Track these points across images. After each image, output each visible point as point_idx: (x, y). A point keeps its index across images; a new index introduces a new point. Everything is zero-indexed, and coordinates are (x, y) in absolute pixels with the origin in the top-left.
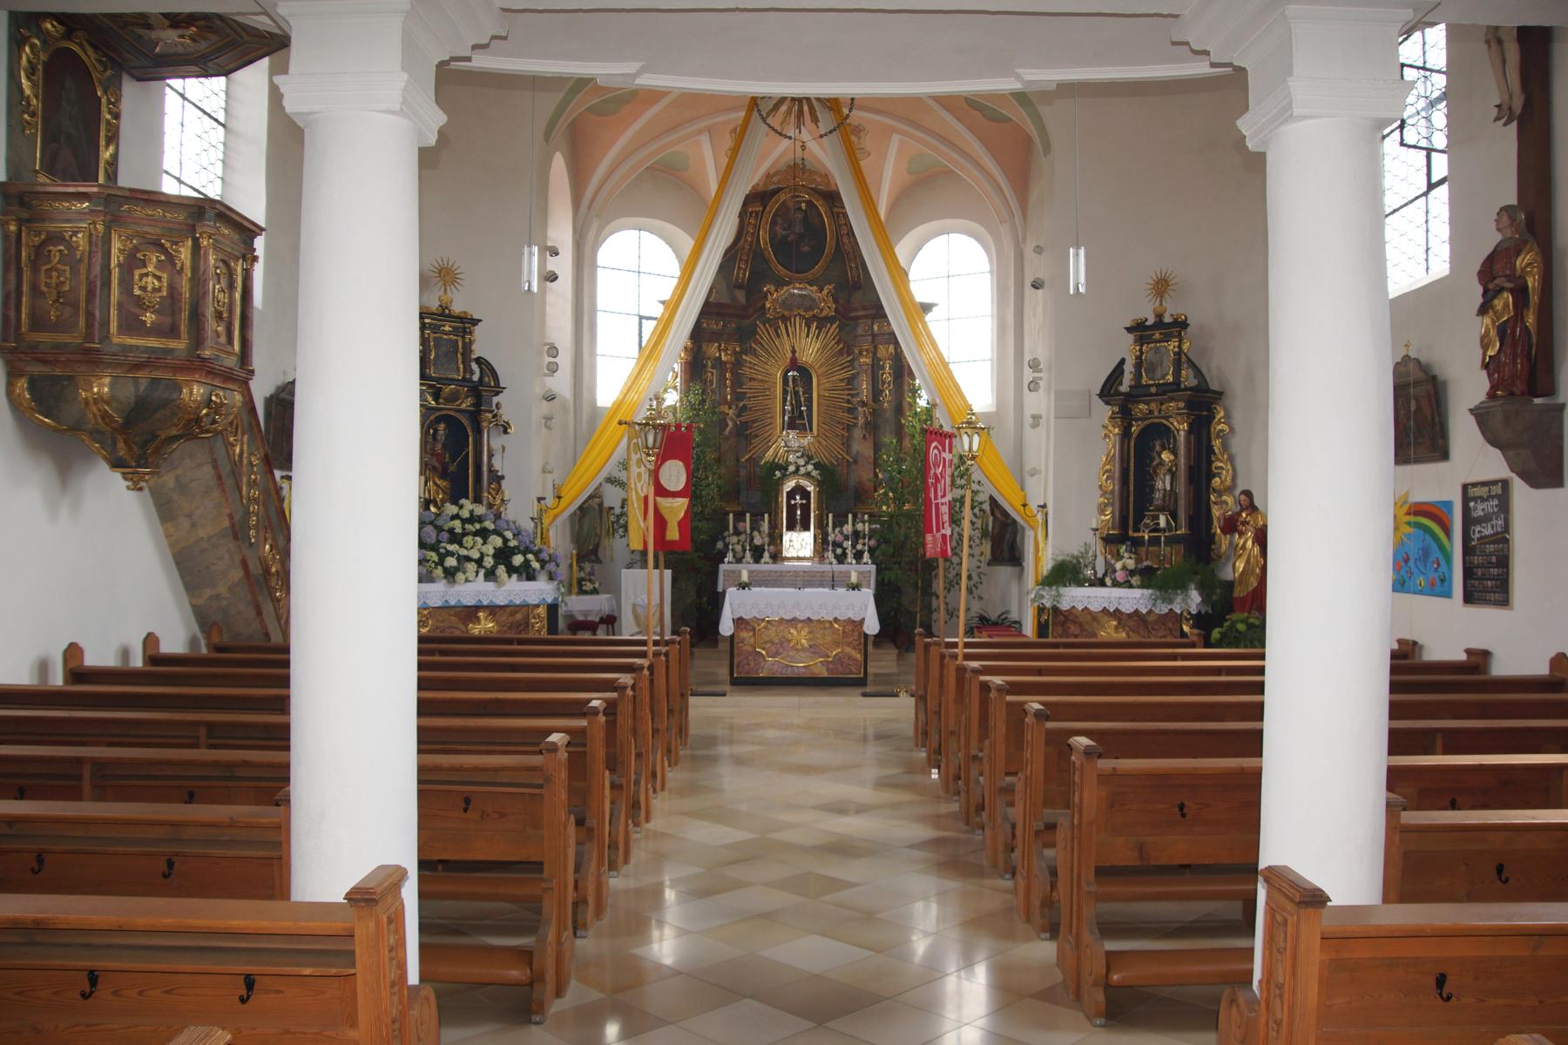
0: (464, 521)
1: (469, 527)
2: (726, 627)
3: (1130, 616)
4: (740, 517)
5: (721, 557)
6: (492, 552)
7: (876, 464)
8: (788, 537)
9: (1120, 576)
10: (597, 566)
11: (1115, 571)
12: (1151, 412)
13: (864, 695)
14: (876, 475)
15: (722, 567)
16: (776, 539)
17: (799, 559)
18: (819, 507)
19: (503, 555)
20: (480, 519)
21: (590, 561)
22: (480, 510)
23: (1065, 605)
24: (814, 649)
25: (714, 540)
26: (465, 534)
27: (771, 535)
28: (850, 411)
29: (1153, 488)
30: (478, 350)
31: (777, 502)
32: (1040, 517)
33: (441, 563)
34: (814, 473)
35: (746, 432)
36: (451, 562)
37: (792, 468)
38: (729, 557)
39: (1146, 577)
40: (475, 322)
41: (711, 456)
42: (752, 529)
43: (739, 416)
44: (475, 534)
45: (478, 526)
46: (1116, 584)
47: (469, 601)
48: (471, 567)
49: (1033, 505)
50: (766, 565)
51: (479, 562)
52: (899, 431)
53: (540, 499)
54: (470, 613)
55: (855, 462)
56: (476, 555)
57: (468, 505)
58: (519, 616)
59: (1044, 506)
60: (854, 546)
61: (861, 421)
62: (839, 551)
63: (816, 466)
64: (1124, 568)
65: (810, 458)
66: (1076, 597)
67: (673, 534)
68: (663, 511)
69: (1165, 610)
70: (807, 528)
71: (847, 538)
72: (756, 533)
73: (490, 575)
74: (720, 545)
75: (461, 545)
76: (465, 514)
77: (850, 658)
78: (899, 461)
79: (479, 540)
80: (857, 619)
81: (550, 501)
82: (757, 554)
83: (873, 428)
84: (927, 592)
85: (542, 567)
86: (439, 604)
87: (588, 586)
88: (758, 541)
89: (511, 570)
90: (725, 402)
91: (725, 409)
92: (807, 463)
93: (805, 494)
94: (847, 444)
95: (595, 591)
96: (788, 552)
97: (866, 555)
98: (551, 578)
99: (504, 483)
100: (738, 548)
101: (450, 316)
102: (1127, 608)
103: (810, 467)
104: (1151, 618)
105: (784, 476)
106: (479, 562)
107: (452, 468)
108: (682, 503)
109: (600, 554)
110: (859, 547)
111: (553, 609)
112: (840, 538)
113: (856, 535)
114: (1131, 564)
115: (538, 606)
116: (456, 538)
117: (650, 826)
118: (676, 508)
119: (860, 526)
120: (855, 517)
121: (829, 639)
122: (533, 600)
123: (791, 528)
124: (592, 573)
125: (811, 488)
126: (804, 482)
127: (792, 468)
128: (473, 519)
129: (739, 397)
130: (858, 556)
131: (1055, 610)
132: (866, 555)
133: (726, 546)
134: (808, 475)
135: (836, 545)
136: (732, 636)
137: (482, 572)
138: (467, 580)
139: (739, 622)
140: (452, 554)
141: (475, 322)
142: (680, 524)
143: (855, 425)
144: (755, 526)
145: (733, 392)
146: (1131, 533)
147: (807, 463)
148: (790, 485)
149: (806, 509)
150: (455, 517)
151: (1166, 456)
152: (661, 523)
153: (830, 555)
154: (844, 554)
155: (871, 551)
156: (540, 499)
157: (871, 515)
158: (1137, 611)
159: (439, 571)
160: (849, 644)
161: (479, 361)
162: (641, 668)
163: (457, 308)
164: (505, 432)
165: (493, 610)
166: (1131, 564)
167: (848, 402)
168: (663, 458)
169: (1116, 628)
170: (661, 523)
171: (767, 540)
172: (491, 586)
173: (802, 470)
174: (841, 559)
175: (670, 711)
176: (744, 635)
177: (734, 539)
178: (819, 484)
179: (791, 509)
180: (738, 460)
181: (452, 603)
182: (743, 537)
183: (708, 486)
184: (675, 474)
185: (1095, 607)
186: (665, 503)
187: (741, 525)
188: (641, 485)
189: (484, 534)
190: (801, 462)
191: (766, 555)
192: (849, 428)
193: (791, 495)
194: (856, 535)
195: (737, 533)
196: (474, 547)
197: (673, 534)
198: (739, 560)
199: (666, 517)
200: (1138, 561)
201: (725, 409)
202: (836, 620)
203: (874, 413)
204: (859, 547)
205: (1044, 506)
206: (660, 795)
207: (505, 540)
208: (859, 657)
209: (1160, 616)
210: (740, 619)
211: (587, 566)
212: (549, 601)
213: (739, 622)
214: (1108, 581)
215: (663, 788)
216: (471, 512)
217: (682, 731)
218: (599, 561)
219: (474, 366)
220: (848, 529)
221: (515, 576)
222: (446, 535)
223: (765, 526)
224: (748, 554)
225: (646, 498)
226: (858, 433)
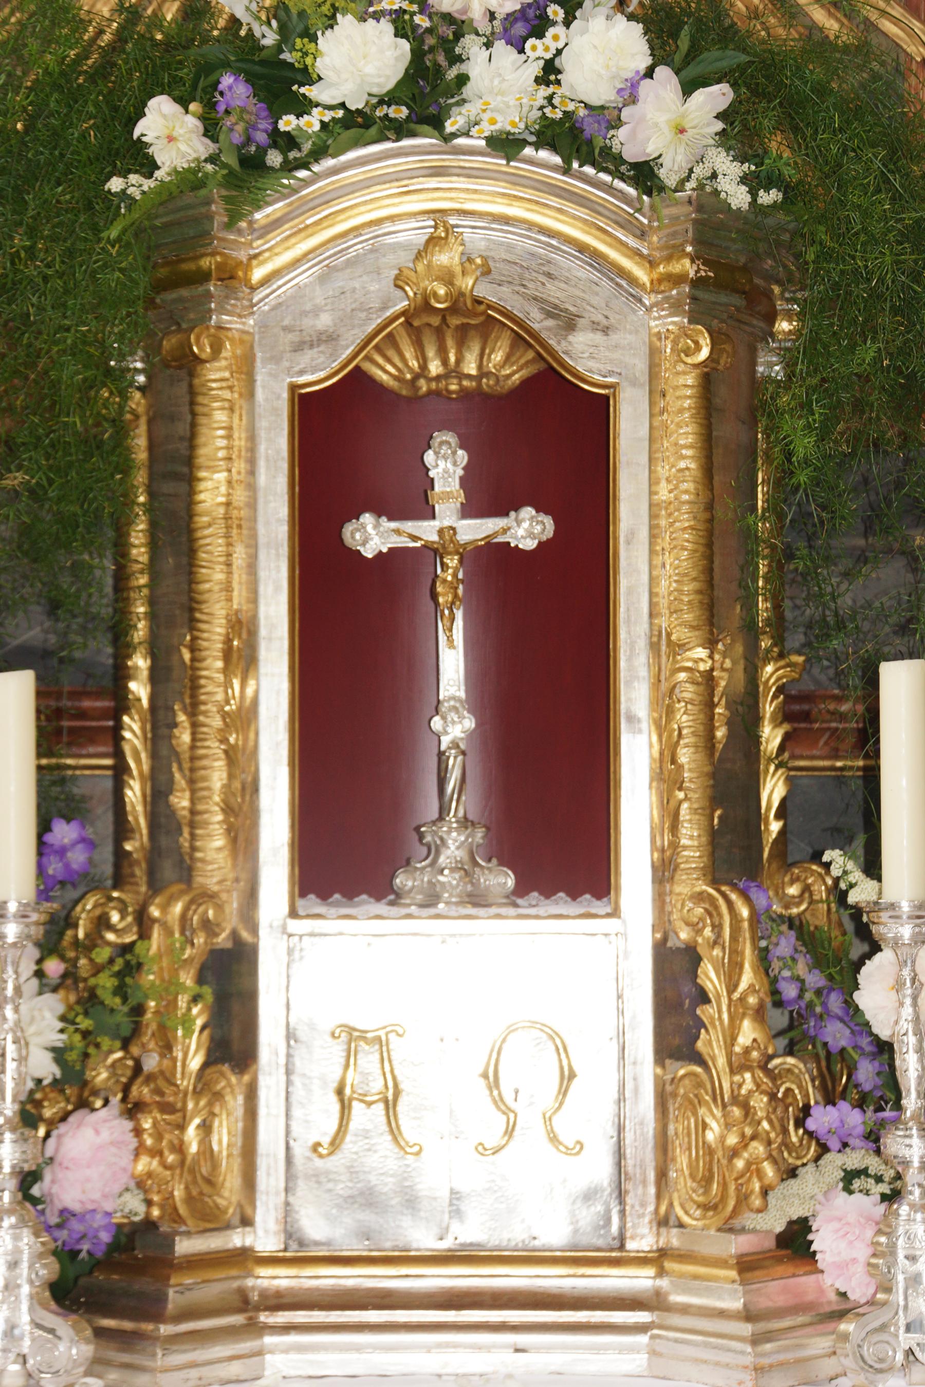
8: (321, 970)
31: (177, 532)
34: (676, 124)
37: (357, 60)
70: (554, 841)
93: (551, 435)
123: (351, 851)
149: (551, 629)
173: (498, 86)
178: (729, 275)
179: (351, 626)
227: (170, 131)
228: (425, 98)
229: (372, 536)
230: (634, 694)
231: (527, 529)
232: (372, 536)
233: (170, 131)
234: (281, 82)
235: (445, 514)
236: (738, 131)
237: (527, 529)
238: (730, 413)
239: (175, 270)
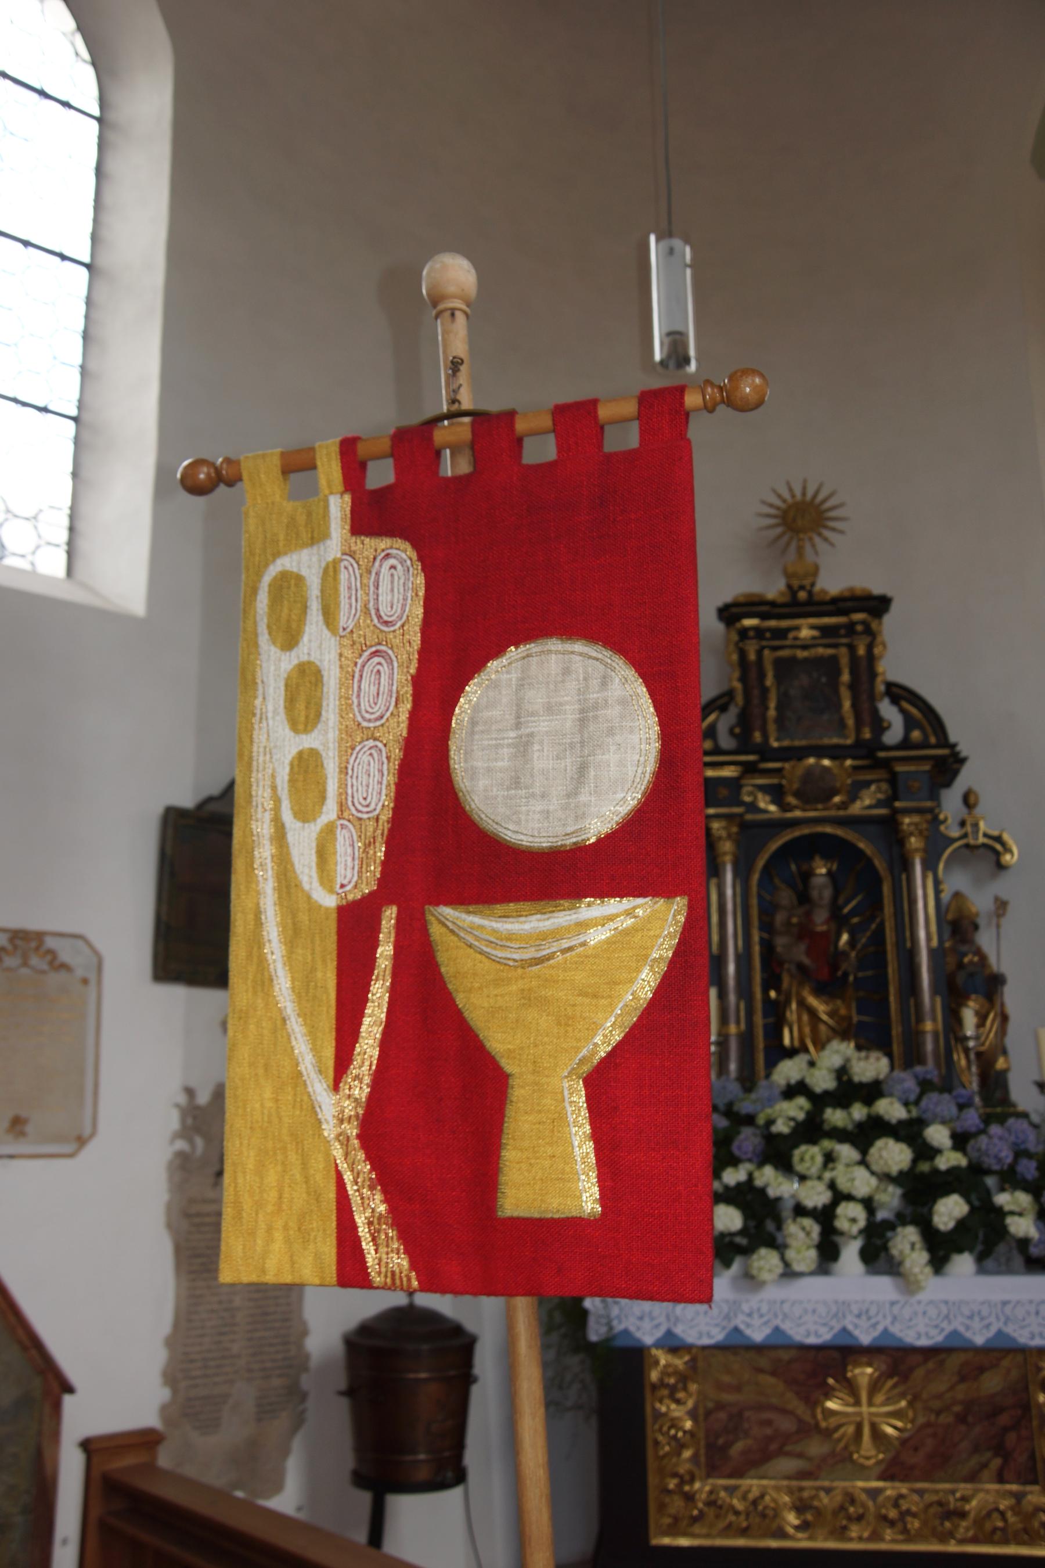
0: (820, 1101)
1: (835, 1117)
20: (872, 1091)
22: (871, 1067)
26: (811, 1130)
30: (892, 667)
40: (879, 605)
45: (859, 1112)
47: (813, 1332)
48: (801, 1238)
51: (825, 1216)
56: (816, 1196)
57: (838, 1052)
58: (992, 1383)
73: (876, 1254)
75: (785, 1166)
76: (823, 1081)
79: (846, 1152)
86: (717, 1336)
101: (810, 601)
128: (848, 1089)
138: (789, 1273)
141: (879, 605)
161: (898, 693)
163: (832, 583)
164: (1000, 867)
172: (883, 1286)
181: (758, 1335)
186: (481, 943)
199: (498, 1041)
207: (925, 1151)
216: (842, 1073)
219: (888, 710)
221: (963, 1263)
222: (747, 1140)
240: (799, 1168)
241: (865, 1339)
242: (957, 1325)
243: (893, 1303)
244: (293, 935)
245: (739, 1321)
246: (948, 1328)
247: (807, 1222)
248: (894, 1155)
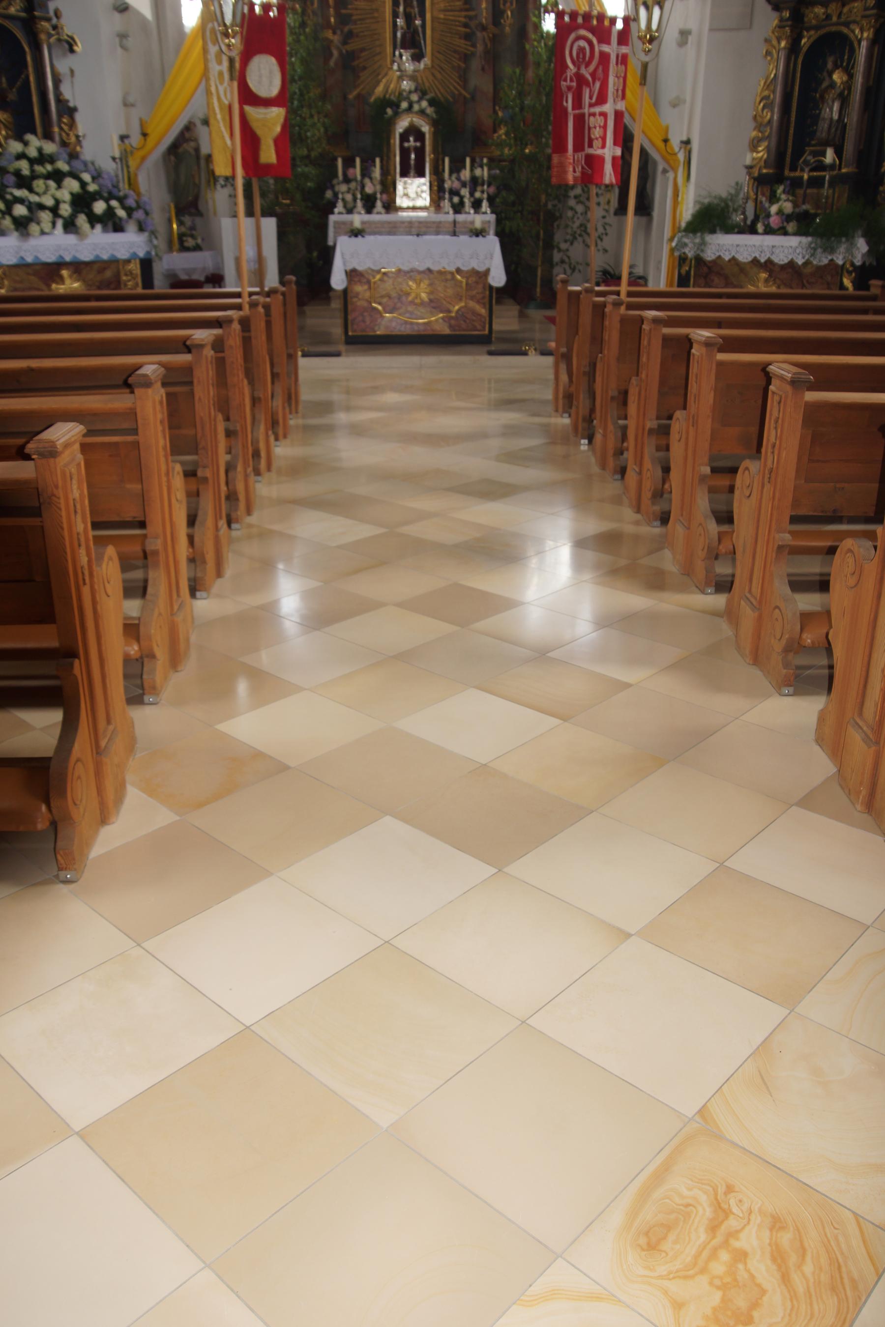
0: (32, 162)
1: (39, 169)
2: (338, 280)
3: (783, 267)
4: (349, 163)
5: (330, 208)
6: (67, 197)
7: (496, 99)
9: (774, 221)
10: (198, 221)
11: (768, 215)
12: (828, 17)
13: (491, 353)
14: (495, 112)
15: (332, 218)
16: (389, 188)
17: (414, 208)
18: (435, 150)
19: (82, 202)
20: (51, 159)
21: (191, 214)
22: (50, 148)
23: (709, 255)
24: (434, 304)
25: (321, 189)
26: (34, 176)
27: (383, 183)
28: (468, 37)
29: (816, 119)
32: (681, 156)
33: (9, 211)
34: (430, 111)
35: (352, 65)
36: (20, 210)
38: (339, 207)
39: (802, 222)
41: (314, 92)
42: (363, 175)
43: (345, 42)
44: (48, 176)
45: (49, 167)
46: (769, 231)
47: (49, 257)
48: (45, 217)
49: (675, 143)
50: (379, 216)
51: (55, 210)
52: (522, 59)
53: (123, 138)
54: (51, 271)
55: (473, 98)
58: (108, 274)
59: (687, 142)
60: (472, 194)
61: (480, 48)
62: (456, 200)
63: (431, 103)
64: (780, 212)
65: (423, 94)
66: (725, 245)
67: (268, 155)
68: (255, 125)
69: (825, 261)
70: (421, 174)
71: (464, 185)
72: (367, 181)
73: (70, 226)
74: (329, 194)
75: (31, 190)
76: (33, 153)
77: (474, 313)
78: (521, 94)
79: (52, 184)
80: (481, 269)
81: (135, 139)
82: (369, 204)
83: (493, 58)
84: (549, 245)
85: (130, 215)
86: (13, 261)
87: (190, 242)
88: (369, 189)
89: (93, 219)
90: (328, 25)
91: (329, 34)
92: (421, 99)
93: (420, 136)
94: (464, 79)
95: (197, 248)
96: (401, 202)
97: (485, 205)
98: (141, 228)
99: (78, 117)
100: (349, 197)
102: (781, 259)
103: (424, 104)
104: (808, 270)
105: (397, 114)
106: (55, 210)
107: (12, 96)
108: (277, 114)
109: (201, 207)
110: (478, 195)
111: (146, 264)
112: (456, 185)
113: (475, 182)
114: (788, 207)
115: (128, 261)
116: (25, 182)
117: (253, 519)
118: (270, 121)
119: (478, 172)
120: (473, 162)
121: (450, 292)
122: (122, 254)
123: (404, 174)
124: (193, 228)
125: (426, 129)
126: (419, 121)
127: (404, 105)
128: (42, 158)
129: (343, 20)
130: (477, 205)
131: (699, 260)
132: (485, 205)
133: (336, 195)
134: (422, 112)
135: (454, 192)
136: (345, 291)
137: (60, 223)
138: (43, 233)
139: (352, 275)
140: (21, 201)
142: (277, 141)
143: (473, 54)
144: (366, 173)
145: (338, 15)
146: (787, 172)
147: (421, 99)
148: (402, 124)
149: (420, 152)
150: (21, 156)
151: (838, 77)
152: (251, 141)
153: (446, 204)
154: (462, 203)
155: (491, 200)
156: (123, 138)
157: (491, 160)
158: (792, 263)
159: (7, 222)
160: (472, 298)
162: (229, 321)
165: (78, 267)
166: (788, 207)
167: (466, 25)
168: (247, 56)
169: (766, 281)
170: (251, 141)
171: (379, 188)
172: (71, 239)
173: (416, 107)
174: (458, 208)
175: (275, 376)
176: (359, 288)
177: (343, 188)
178: (434, 123)
179: (405, 153)
180: (345, 98)
181: (29, 259)
182: (353, 185)
183: (314, 125)
184: (266, 76)
185: (744, 257)
187: (351, 171)
188: (226, 92)
189: (58, 177)
190: (414, 97)
191: (379, 204)
192: (466, 58)
193: (404, 137)
194: (475, 182)
195: (347, 180)
196: (47, 193)
197: (268, 155)
198: (350, 211)
199: (259, 132)
200: (795, 205)
201: (329, 34)
202: (458, 271)
203: (494, 39)
204: (478, 195)
205: (687, 142)
206: (266, 475)
207: (83, 185)
208: (484, 312)
209: (819, 268)
210: (354, 271)
211: (187, 220)
212: (141, 254)
213: (352, 275)
214: (760, 227)
215: (269, 469)
216: (40, 150)
217: (291, 398)
218: (200, 214)
220: (466, 174)
221: (99, 227)
223: (377, 173)
224: (359, 204)
225: (230, 107)
226: (476, 64)
227: (389, 111)
228: (410, 107)
229: (406, 145)
230: (427, 159)
231: (418, 144)
232: (406, 145)
233: (389, 111)
234: (398, 106)
235: (412, 142)
236: (436, 112)
237: (418, 144)
238: (435, 135)
239: (391, 123)
240: (36, 189)
241: (68, 259)
242: (98, 252)
243: (75, 245)
244: (221, 108)
245: (22, 254)
246: (95, 253)
247: (47, 212)
248: (72, 185)
